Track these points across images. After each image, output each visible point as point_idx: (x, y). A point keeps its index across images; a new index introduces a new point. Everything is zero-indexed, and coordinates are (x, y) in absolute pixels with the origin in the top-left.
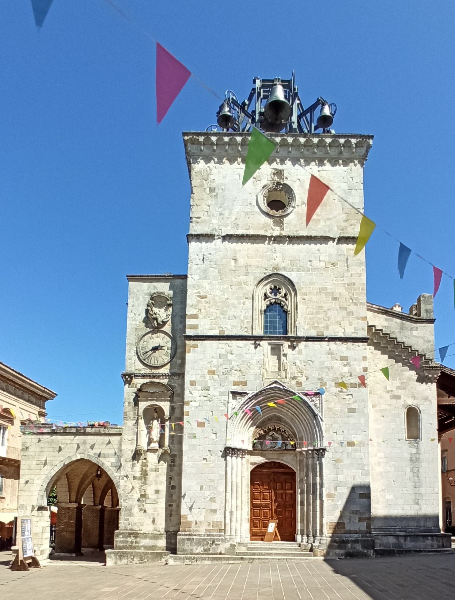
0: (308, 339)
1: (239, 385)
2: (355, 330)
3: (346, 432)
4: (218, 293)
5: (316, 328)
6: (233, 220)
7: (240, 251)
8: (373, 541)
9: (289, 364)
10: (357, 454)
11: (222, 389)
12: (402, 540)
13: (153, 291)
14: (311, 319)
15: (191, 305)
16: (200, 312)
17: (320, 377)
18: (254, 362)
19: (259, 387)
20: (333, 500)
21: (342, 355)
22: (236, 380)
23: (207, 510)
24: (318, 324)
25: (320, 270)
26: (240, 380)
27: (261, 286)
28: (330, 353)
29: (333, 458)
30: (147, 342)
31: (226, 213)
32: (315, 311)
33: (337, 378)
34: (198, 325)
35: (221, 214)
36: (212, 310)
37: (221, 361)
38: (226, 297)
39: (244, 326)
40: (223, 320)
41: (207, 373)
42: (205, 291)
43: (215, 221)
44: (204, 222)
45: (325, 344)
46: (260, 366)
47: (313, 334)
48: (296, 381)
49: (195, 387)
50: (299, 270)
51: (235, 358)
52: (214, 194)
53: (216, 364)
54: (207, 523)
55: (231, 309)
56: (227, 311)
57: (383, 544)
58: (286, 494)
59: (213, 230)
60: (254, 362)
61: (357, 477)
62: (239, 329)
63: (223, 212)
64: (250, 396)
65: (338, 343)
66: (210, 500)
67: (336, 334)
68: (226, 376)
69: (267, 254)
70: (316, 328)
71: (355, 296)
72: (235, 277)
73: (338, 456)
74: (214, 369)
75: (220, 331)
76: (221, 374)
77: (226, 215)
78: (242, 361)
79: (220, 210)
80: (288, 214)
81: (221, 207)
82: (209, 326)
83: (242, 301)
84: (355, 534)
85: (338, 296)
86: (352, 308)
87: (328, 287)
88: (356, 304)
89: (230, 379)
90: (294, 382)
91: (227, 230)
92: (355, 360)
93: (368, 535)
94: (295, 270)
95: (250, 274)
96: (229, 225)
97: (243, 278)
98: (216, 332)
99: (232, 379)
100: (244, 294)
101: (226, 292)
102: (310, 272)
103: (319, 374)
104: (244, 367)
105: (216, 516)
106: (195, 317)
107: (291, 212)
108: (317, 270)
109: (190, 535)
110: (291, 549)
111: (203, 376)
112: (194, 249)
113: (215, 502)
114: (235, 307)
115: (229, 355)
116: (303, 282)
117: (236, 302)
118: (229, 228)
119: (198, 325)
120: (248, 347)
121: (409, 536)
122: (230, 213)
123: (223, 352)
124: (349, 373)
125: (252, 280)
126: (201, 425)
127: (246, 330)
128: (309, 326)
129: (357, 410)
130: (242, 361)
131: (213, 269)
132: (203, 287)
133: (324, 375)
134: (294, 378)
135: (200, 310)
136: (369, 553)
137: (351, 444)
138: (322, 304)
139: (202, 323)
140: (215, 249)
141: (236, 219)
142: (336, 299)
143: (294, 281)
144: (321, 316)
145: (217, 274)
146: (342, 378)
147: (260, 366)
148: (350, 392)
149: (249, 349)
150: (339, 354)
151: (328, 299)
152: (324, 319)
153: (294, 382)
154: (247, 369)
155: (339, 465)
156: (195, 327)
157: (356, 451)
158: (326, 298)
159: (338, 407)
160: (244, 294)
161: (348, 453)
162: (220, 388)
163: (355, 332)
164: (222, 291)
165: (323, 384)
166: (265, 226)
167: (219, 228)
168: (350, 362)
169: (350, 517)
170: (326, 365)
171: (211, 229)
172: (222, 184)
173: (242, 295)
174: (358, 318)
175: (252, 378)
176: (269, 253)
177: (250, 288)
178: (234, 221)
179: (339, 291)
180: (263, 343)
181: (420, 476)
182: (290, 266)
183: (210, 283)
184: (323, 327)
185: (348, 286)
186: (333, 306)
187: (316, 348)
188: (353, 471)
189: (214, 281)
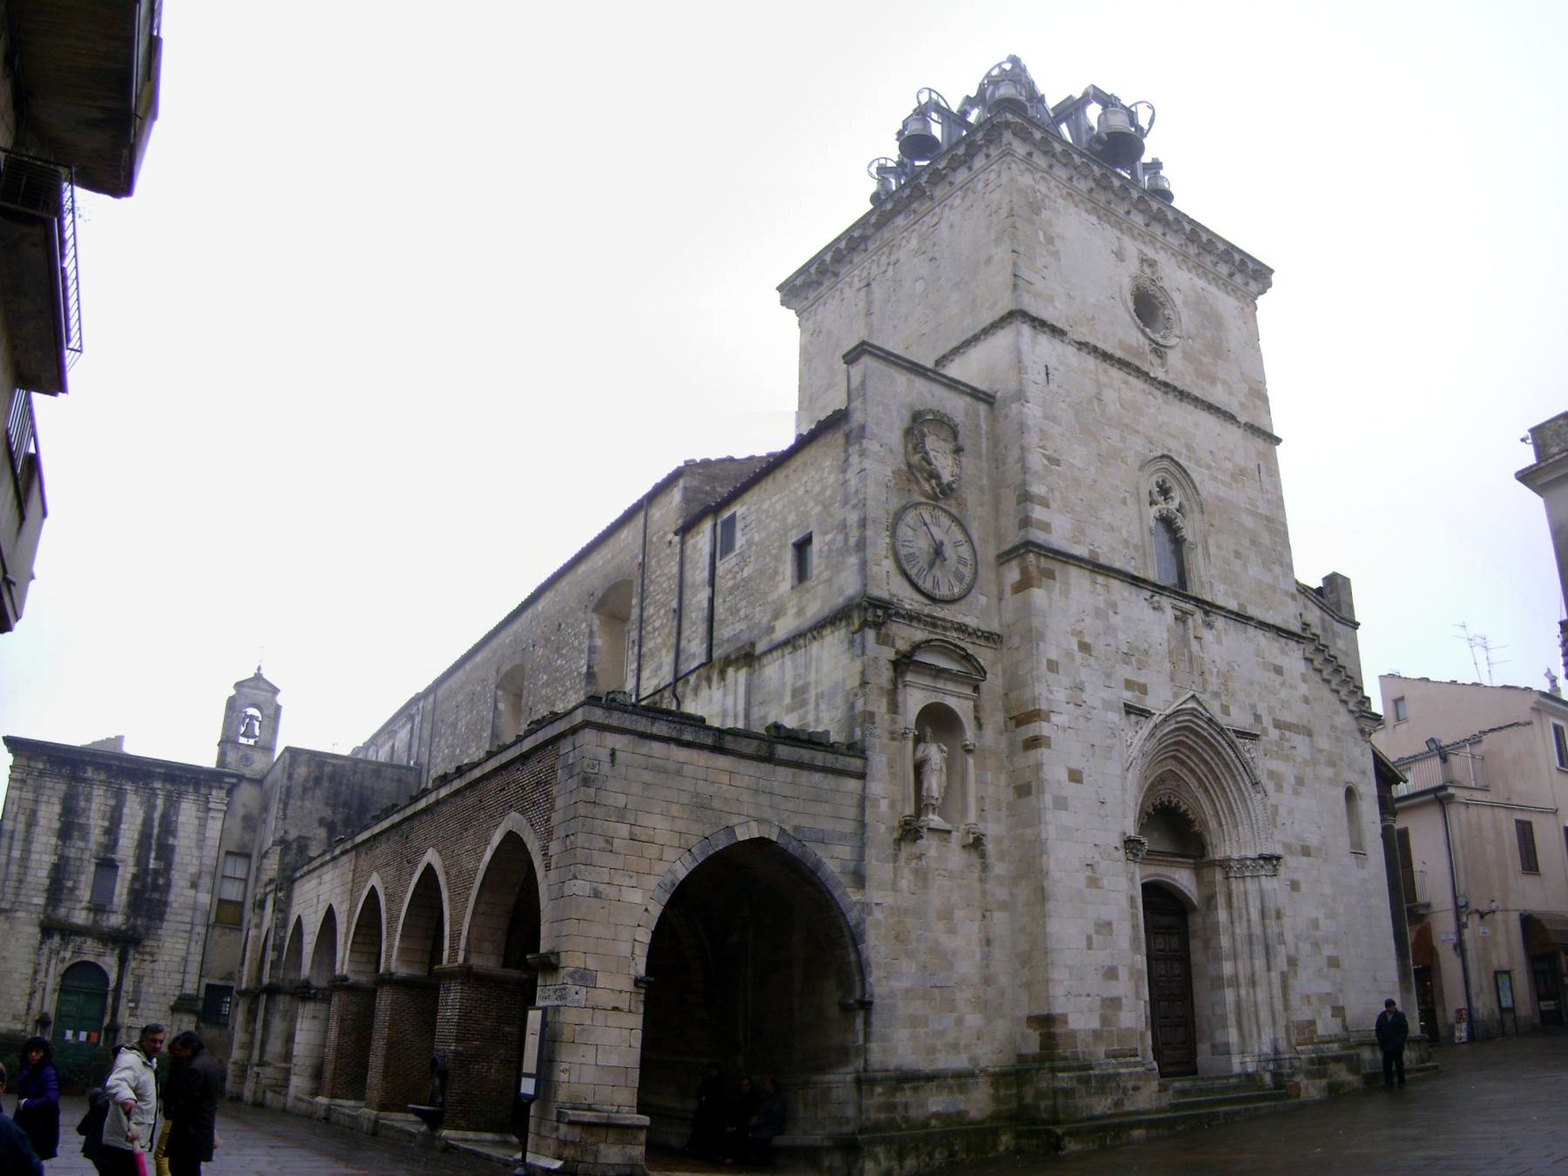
11: (1107, 694)
23: (1104, 1000)
99: (1125, 672)
134: (1216, 695)
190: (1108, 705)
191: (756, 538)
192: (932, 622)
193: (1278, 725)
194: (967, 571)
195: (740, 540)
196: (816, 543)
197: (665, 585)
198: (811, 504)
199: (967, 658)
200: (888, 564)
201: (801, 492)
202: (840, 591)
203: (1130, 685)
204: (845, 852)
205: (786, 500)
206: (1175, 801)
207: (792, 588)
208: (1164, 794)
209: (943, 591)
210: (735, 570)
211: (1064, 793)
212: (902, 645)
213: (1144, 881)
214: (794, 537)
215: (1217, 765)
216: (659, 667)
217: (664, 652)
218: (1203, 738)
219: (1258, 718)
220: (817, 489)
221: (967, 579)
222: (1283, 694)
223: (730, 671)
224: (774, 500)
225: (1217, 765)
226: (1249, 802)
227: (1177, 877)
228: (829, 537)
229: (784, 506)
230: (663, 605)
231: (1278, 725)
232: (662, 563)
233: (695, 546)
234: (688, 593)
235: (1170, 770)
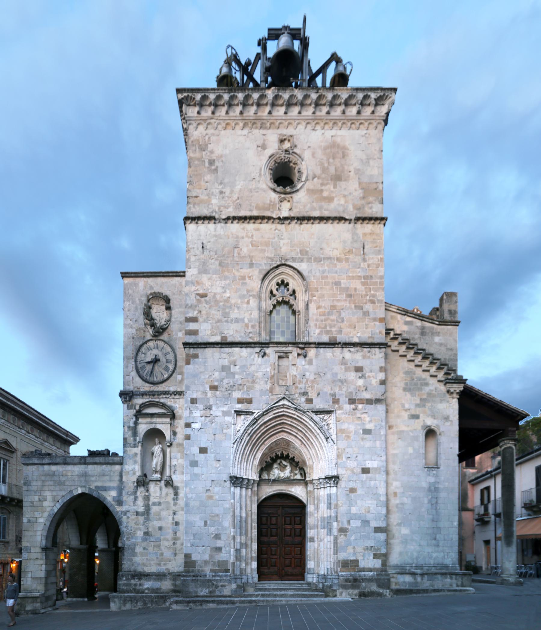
0: (319, 345)
1: (243, 403)
2: (372, 335)
3: (360, 458)
4: (219, 290)
5: (327, 332)
6: (235, 200)
7: (243, 238)
8: (389, 580)
9: (298, 376)
10: (372, 483)
11: (225, 408)
12: (419, 579)
13: (149, 292)
14: (322, 321)
15: (190, 305)
16: (201, 314)
17: (332, 392)
18: (259, 374)
19: (266, 405)
20: (345, 535)
21: (357, 365)
22: (240, 397)
24: (331, 327)
25: (333, 260)
26: (245, 397)
27: (266, 282)
28: (343, 362)
29: (346, 487)
30: (145, 354)
31: (227, 191)
32: (327, 311)
33: (351, 393)
34: (198, 330)
35: (221, 192)
36: (213, 312)
37: (224, 374)
38: (227, 295)
39: (249, 331)
40: (225, 323)
41: (208, 389)
42: (205, 288)
43: (214, 201)
44: (202, 202)
45: (337, 351)
46: (267, 380)
47: (325, 339)
48: (306, 397)
49: (197, 405)
50: (309, 260)
51: (238, 371)
52: (213, 167)
53: (218, 378)
55: (234, 310)
56: (229, 312)
57: (399, 582)
58: (295, 529)
59: (212, 212)
60: (259, 374)
61: (371, 508)
62: (243, 334)
63: (224, 190)
64: (256, 416)
65: (352, 349)
66: (214, 537)
67: (351, 339)
68: (229, 392)
69: (274, 241)
70: (327, 332)
71: (372, 292)
72: (238, 270)
73: (352, 485)
74: (216, 384)
75: (222, 337)
76: (224, 390)
77: (227, 194)
78: (246, 374)
79: (220, 187)
80: (297, 191)
81: (221, 183)
82: (210, 332)
83: (246, 300)
84: (369, 573)
85: (353, 293)
86: (368, 307)
87: (342, 281)
88: (373, 302)
89: (234, 396)
90: (303, 399)
91: (229, 212)
92: (371, 371)
93: (383, 573)
94: (305, 260)
95: (254, 265)
96: (230, 206)
97: (246, 271)
98: (217, 339)
100: (248, 291)
101: (229, 289)
102: (322, 262)
103: (331, 389)
104: (248, 381)
105: (222, 555)
106: (194, 320)
107: (301, 188)
108: (329, 261)
109: (194, 576)
110: (299, 590)
111: (205, 393)
112: (192, 236)
113: (220, 539)
114: (238, 308)
115: (232, 366)
116: (314, 276)
117: (239, 301)
118: (231, 209)
119: (198, 330)
120: (252, 357)
121: (426, 574)
122: (232, 192)
123: (226, 363)
124: (364, 386)
125: (257, 275)
126: (203, 450)
127: (251, 335)
128: (320, 330)
129: (373, 431)
130: (246, 374)
131: (213, 261)
132: (202, 283)
133: (337, 390)
135: (200, 312)
136: (385, 593)
137: (365, 471)
138: (336, 303)
139: (202, 328)
140: (215, 236)
141: (238, 198)
142: (350, 296)
143: (305, 274)
144: (333, 317)
145: (218, 267)
146: (356, 393)
147: (267, 380)
148: (365, 409)
149: (254, 360)
150: (354, 364)
151: (342, 296)
152: (337, 321)
153: (303, 399)
154: (252, 383)
155: (352, 495)
156: (195, 333)
157: (371, 479)
158: (340, 294)
159: (352, 428)
160: (248, 291)
161: (362, 481)
162: (223, 407)
163: (371, 337)
164: (223, 288)
165: (336, 401)
166: (271, 206)
167: (219, 209)
168: (365, 374)
169: (364, 554)
170: (339, 378)
171: (211, 210)
172: (221, 156)
173: (245, 293)
174: (375, 320)
175: (258, 394)
176: (276, 239)
177: (255, 284)
178: (236, 200)
179: (354, 287)
180: (269, 351)
181: (438, 508)
182: (299, 255)
183: (210, 279)
184: (336, 331)
185: (364, 279)
186: (348, 304)
187: (328, 357)
188: (367, 502)
189: (214, 276)
190: (225, 414)
199: (163, 406)
203: (240, 401)
204: (114, 493)
206: (285, 453)
208: (279, 451)
211: (196, 459)
215: (306, 431)
218: (295, 419)
225: (306, 431)
226: (324, 448)
227: (290, 489)
235: (282, 438)
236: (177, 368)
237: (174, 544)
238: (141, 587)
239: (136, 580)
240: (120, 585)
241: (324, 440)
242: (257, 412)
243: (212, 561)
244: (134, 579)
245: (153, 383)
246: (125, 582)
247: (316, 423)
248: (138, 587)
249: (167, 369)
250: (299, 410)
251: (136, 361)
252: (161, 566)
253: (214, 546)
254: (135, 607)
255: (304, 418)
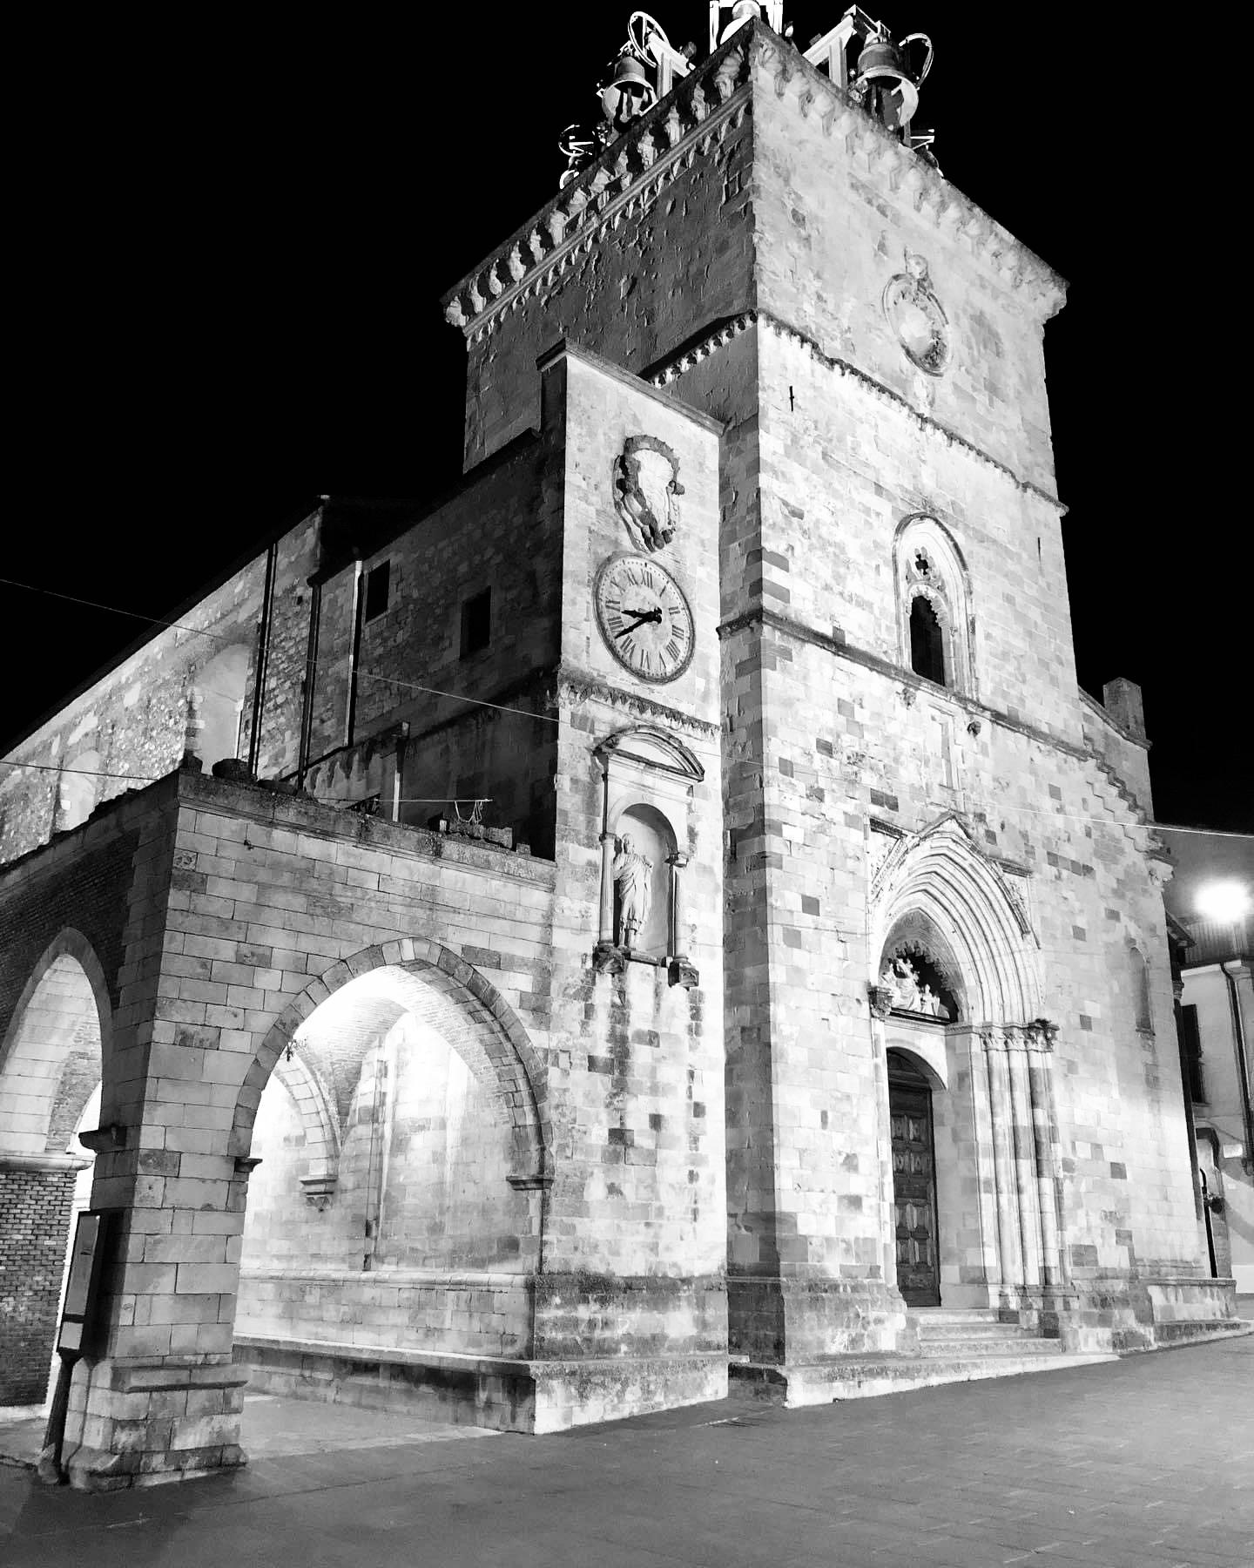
11: (850, 807)
49: (793, 780)
54: (844, 1245)
66: (844, 1163)
99: (869, 780)
162: (845, 802)
190: (851, 821)
191: (415, 594)
192: (642, 704)
193: (1053, 859)
194: (682, 646)
195: (394, 598)
196: (496, 602)
197: (292, 651)
198: (490, 552)
199: (685, 754)
200: (591, 628)
201: (478, 534)
202: (526, 660)
203: (877, 799)
205: (456, 546)
207: (462, 658)
209: (655, 669)
210: (386, 634)
212: (603, 732)
213: (890, 1045)
214: (466, 594)
216: (282, 753)
217: (288, 734)
219: (1030, 852)
220: (499, 532)
221: (682, 655)
222: (1059, 820)
223: (376, 758)
224: (441, 545)
228: (510, 595)
229: (455, 554)
230: (288, 677)
231: (1053, 859)
232: (290, 624)
233: (334, 601)
234: (321, 663)
236: (695, 657)
237: (692, 1176)
238: (607, 1334)
239: (595, 1307)
240: (543, 1324)
241: (1018, 933)
242: (910, 835)
243: (844, 1241)
244: (586, 1301)
245: (641, 676)
246: (560, 1313)
247: (1006, 892)
248: (598, 1334)
249: (672, 650)
250: (979, 852)
251: (596, 595)
252: (657, 1254)
253: (845, 1192)
254: (614, 1409)
255: (983, 872)
